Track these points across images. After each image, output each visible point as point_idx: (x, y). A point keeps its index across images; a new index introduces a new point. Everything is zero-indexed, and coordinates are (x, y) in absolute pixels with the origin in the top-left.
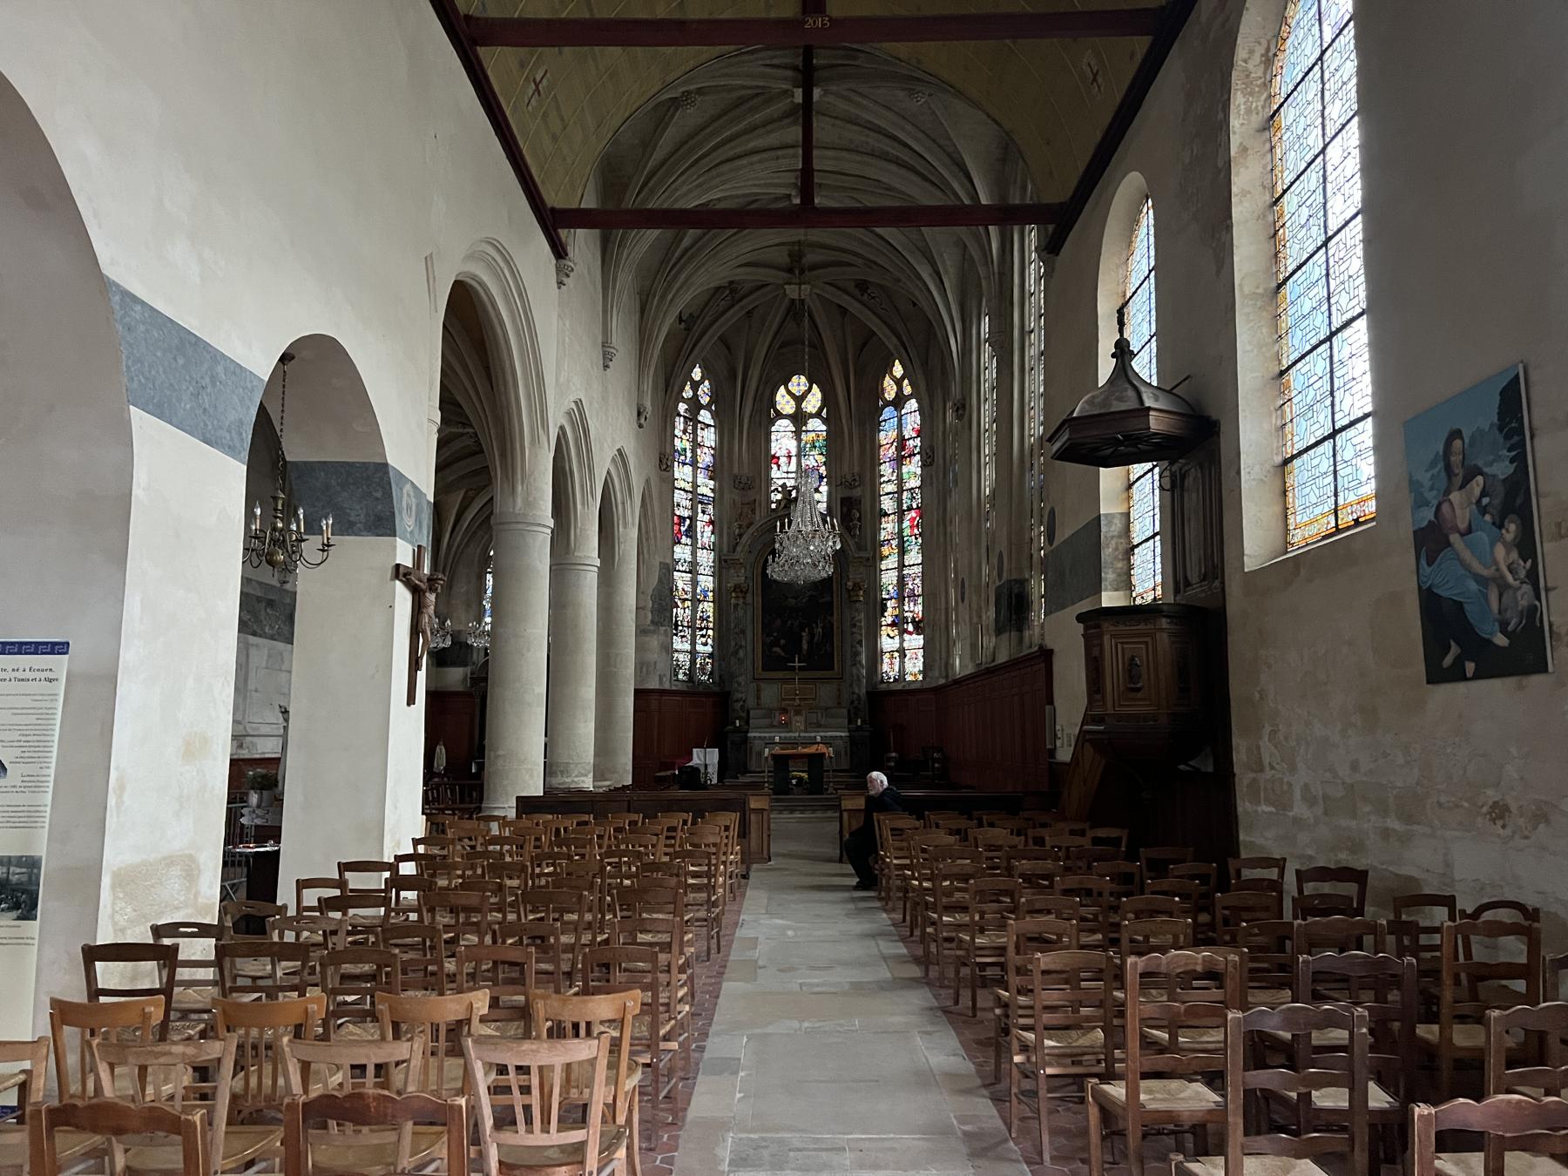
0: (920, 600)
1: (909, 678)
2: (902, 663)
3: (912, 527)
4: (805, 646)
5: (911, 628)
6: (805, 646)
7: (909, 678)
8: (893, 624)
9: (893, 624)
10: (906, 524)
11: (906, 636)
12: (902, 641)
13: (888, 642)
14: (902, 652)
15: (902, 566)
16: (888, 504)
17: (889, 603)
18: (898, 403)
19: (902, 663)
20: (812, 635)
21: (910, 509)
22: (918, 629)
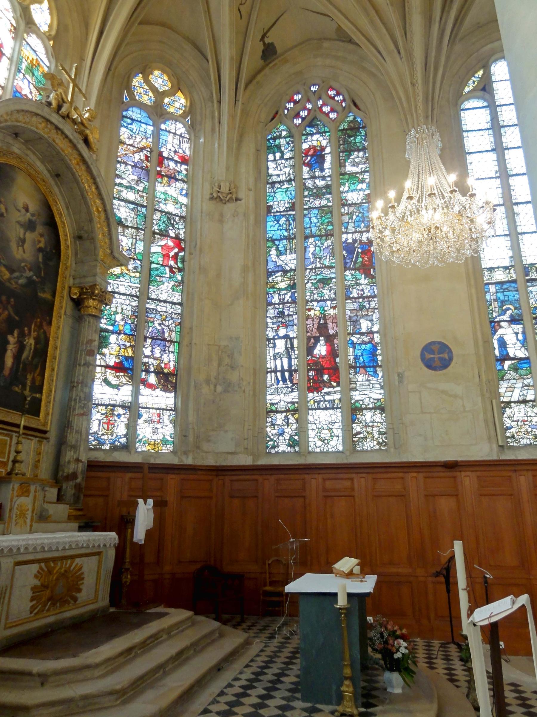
0: (173, 348)
1: (140, 448)
2: (132, 426)
3: (166, 256)
4: (9, 361)
5: (152, 379)
6: (9, 361)
7: (140, 448)
8: (118, 368)
9: (118, 368)
10: (155, 249)
11: (144, 391)
12: (136, 394)
13: (101, 392)
14: (133, 409)
15: (143, 296)
16: (123, 212)
17: (113, 338)
18: (158, 113)
19: (132, 426)
20: (21, 347)
21: (164, 234)
22: (167, 380)
